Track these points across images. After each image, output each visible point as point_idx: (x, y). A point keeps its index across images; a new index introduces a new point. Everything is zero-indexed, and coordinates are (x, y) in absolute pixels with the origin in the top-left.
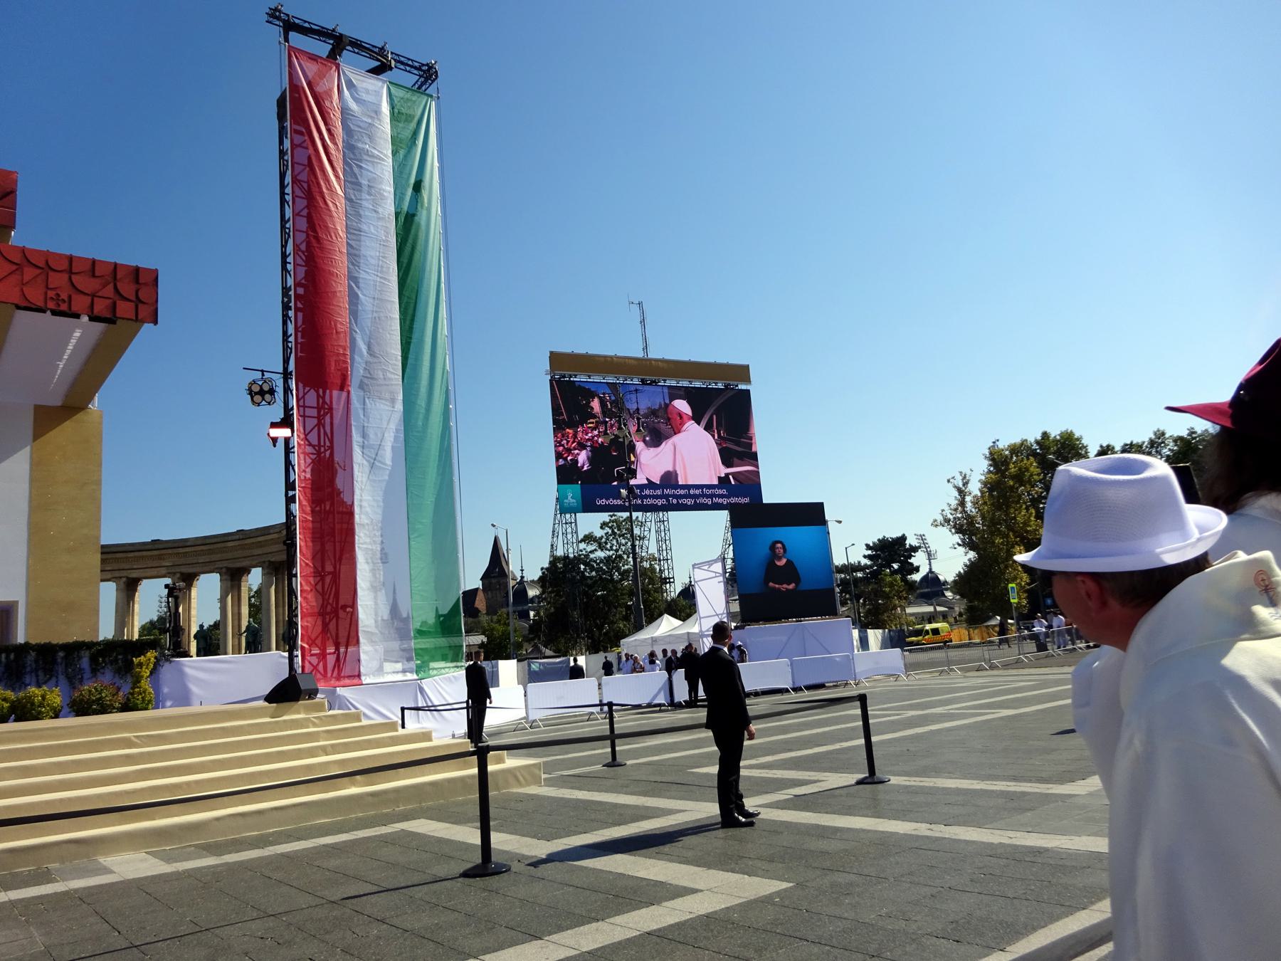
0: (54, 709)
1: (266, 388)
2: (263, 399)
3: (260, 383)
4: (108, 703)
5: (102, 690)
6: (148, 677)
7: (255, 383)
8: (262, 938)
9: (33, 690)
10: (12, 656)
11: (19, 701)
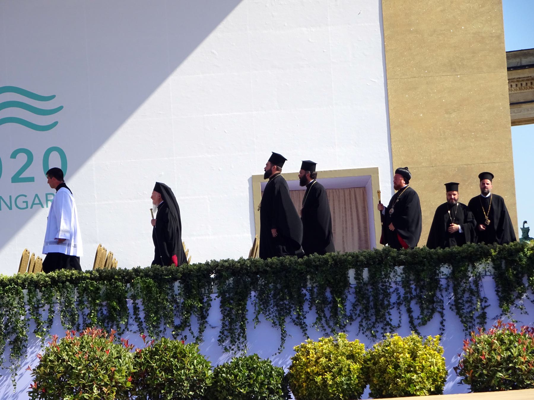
4: (524, 367)
5: (511, 342)
10: (365, 273)
11: (374, 359)
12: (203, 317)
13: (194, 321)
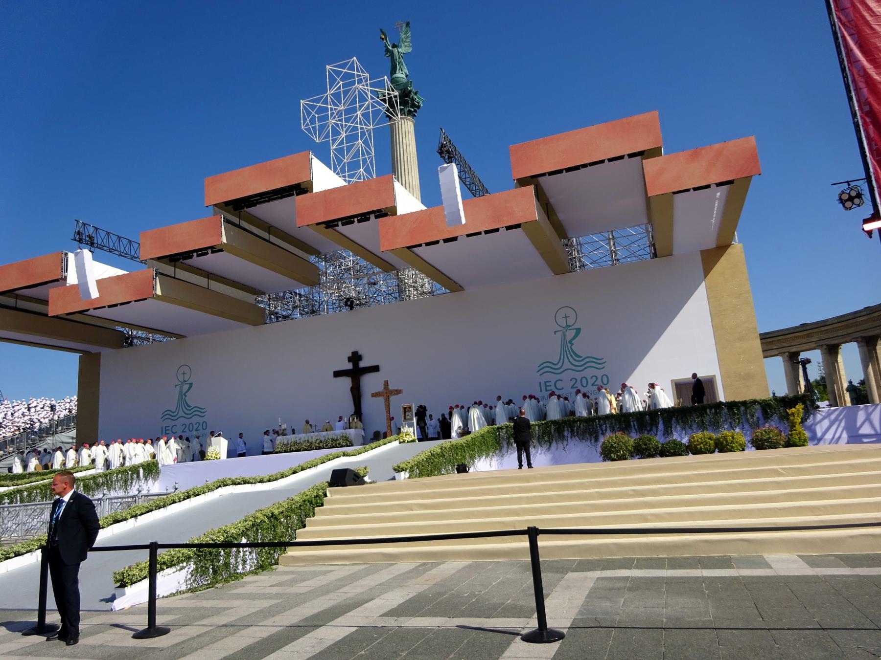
0: (740, 445)
1: (853, 194)
2: (853, 203)
3: (848, 192)
4: (775, 441)
7: (843, 193)
8: (874, 654)
12: (657, 427)
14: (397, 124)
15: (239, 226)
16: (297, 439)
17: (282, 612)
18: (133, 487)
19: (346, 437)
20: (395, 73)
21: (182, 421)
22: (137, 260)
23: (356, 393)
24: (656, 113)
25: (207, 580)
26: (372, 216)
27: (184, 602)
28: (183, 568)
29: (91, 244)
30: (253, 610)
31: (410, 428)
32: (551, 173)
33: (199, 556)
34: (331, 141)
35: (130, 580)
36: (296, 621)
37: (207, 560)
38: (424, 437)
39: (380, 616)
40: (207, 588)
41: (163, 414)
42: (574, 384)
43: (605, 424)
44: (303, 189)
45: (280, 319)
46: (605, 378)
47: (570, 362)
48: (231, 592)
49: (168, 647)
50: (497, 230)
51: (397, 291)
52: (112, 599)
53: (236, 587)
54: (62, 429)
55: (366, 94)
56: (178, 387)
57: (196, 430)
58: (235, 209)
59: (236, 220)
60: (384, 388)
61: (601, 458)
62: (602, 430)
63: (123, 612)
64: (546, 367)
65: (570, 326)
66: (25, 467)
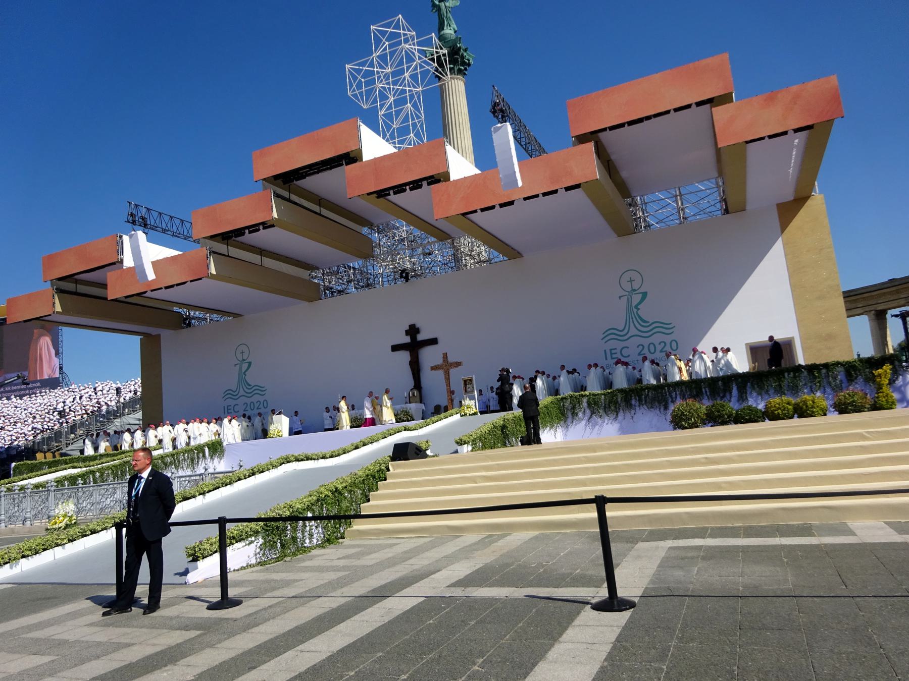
0: (822, 409)
4: (860, 404)
6: (888, 385)
9: (808, 397)
12: (731, 393)
13: (728, 395)
14: (447, 84)
15: (289, 200)
16: (358, 415)
17: (350, 584)
18: (199, 466)
19: (406, 412)
20: (443, 29)
21: (243, 400)
22: (190, 239)
23: (415, 367)
24: (726, 56)
25: (276, 554)
26: (425, 183)
27: (255, 574)
28: (252, 542)
29: (145, 225)
30: (322, 582)
31: (472, 401)
32: (612, 128)
33: (267, 530)
34: (379, 107)
35: (202, 554)
36: (364, 592)
37: (274, 535)
38: (485, 410)
39: (448, 586)
40: (276, 562)
41: (224, 393)
42: (641, 351)
43: (675, 391)
44: (353, 158)
45: (335, 294)
46: (674, 344)
47: (637, 328)
48: (299, 565)
49: (241, 618)
50: (555, 192)
51: (453, 261)
52: (186, 572)
53: (304, 560)
54: (128, 411)
55: (413, 53)
56: (238, 366)
57: (258, 409)
58: (285, 183)
59: (286, 194)
60: (444, 361)
61: (671, 427)
62: (671, 397)
63: (196, 585)
64: (611, 334)
65: (635, 290)
66: (96, 449)
